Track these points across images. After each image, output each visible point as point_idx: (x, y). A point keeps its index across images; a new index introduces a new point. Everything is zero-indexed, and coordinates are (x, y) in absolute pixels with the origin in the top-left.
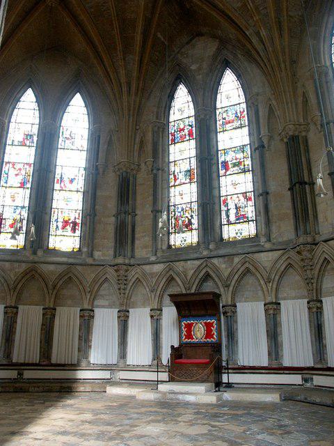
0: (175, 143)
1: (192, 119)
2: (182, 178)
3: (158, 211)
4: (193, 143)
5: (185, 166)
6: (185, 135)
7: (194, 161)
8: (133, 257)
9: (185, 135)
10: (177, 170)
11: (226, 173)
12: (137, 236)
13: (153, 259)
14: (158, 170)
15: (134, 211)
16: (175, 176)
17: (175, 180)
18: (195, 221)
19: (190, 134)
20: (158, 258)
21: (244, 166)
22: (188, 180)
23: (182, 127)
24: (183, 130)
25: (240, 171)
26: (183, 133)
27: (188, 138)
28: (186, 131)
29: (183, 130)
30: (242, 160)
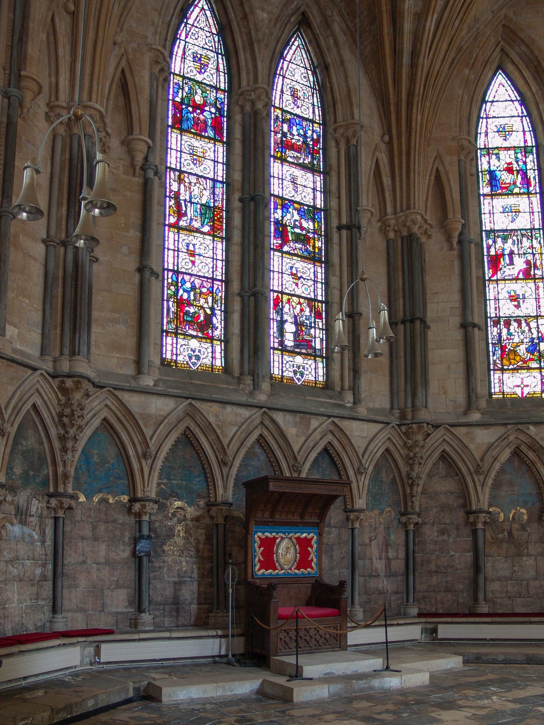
10: (184, 196)
11: (281, 246)
16: (178, 205)
18: (218, 321)
21: (314, 247)
22: (206, 229)
25: (306, 254)
30: (311, 236)
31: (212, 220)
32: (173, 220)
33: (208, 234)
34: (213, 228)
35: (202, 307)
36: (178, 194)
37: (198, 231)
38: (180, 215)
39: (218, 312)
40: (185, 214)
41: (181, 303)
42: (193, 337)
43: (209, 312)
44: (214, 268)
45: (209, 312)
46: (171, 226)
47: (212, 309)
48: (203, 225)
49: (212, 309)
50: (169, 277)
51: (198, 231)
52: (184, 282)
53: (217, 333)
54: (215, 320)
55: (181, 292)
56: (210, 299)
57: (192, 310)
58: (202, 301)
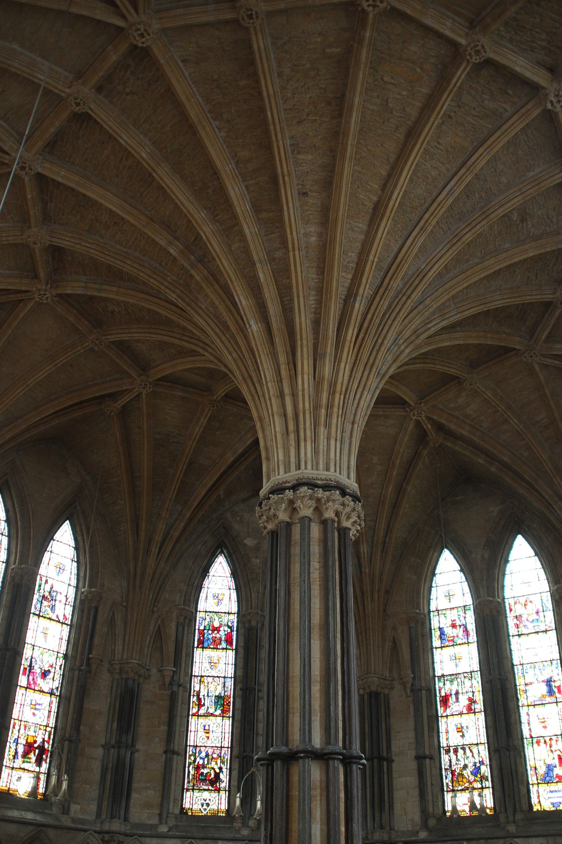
0: (203, 648)
1: (234, 618)
2: (209, 703)
3: (174, 753)
4: (231, 654)
5: (216, 689)
6: (220, 639)
7: (230, 683)
8: (126, 819)
9: (220, 639)
10: (203, 693)
12: (135, 785)
13: (164, 829)
14: (179, 686)
15: (133, 745)
16: (199, 700)
17: (200, 705)
18: (224, 777)
19: (229, 640)
20: (170, 829)
22: (218, 712)
23: (216, 624)
24: (217, 629)
26: (218, 636)
27: (224, 645)
28: (222, 634)
29: (217, 629)
31: (223, 705)
32: (195, 710)
33: (220, 716)
34: (223, 711)
35: (213, 769)
36: (199, 693)
37: (212, 715)
38: (200, 705)
39: (224, 770)
40: (204, 705)
41: (197, 768)
42: (205, 790)
43: (218, 771)
44: (223, 739)
45: (218, 771)
46: (193, 715)
47: (220, 769)
48: (216, 710)
49: (220, 769)
50: (190, 751)
51: (212, 715)
52: (200, 752)
53: (223, 785)
54: (221, 776)
55: (198, 759)
56: (219, 761)
57: (205, 771)
58: (213, 763)
